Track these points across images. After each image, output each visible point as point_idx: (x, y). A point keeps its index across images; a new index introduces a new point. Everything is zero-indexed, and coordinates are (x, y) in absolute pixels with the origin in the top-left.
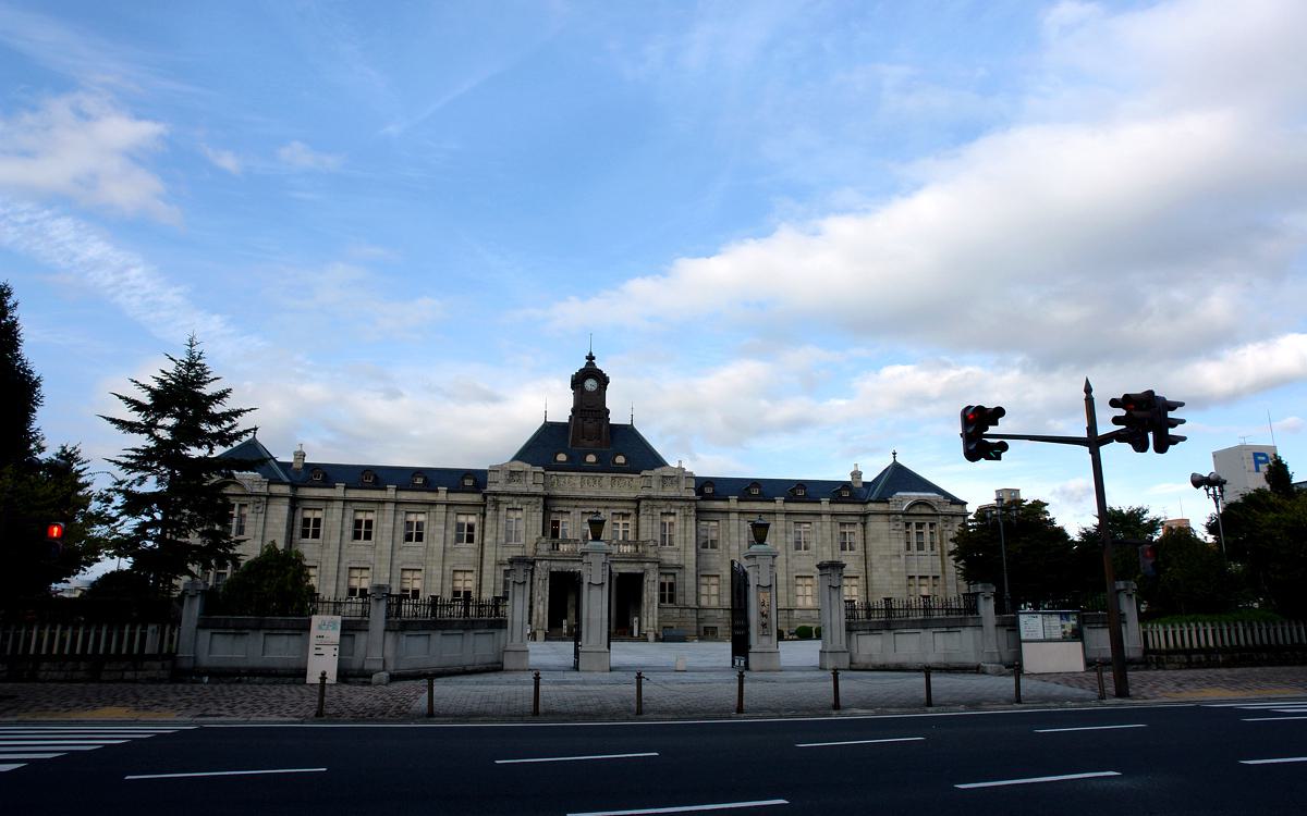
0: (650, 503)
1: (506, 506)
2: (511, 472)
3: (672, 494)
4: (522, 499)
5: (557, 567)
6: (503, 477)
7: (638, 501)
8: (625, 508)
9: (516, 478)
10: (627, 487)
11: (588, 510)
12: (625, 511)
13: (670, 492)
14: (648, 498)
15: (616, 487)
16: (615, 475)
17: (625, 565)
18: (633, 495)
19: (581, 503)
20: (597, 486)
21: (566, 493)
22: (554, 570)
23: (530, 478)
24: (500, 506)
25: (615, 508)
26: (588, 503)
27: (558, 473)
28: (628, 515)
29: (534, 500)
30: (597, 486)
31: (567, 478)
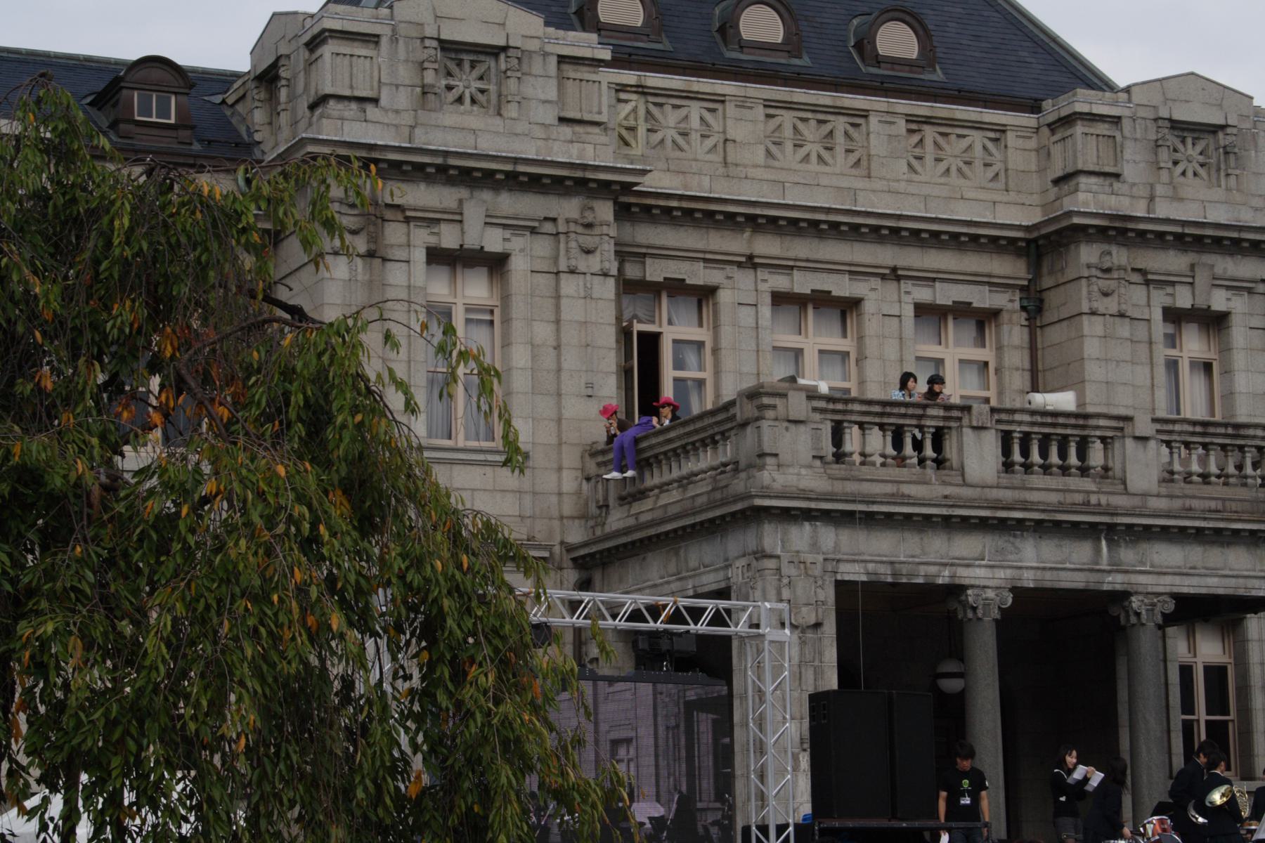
0: (1120, 256)
1: (423, 237)
2: (446, 46)
3: (1219, 215)
4: (510, 203)
5: (874, 555)
6: (405, 74)
7: (1044, 247)
8: (975, 280)
9: (466, 82)
10: (980, 174)
11: (803, 284)
12: (981, 298)
13: (1202, 203)
14: (1118, 231)
15: (929, 171)
16: (922, 108)
17: (1195, 554)
18: (1018, 213)
19: (767, 246)
20: (840, 161)
21: (701, 186)
22: (854, 573)
23: (540, 87)
24: (394, 233)
25: (929, 279)
26: (802, 248)
27: (655, 80)
28: (983, 319)
29: (568, 208)
30: (840, 161)
31: (695, 110)
